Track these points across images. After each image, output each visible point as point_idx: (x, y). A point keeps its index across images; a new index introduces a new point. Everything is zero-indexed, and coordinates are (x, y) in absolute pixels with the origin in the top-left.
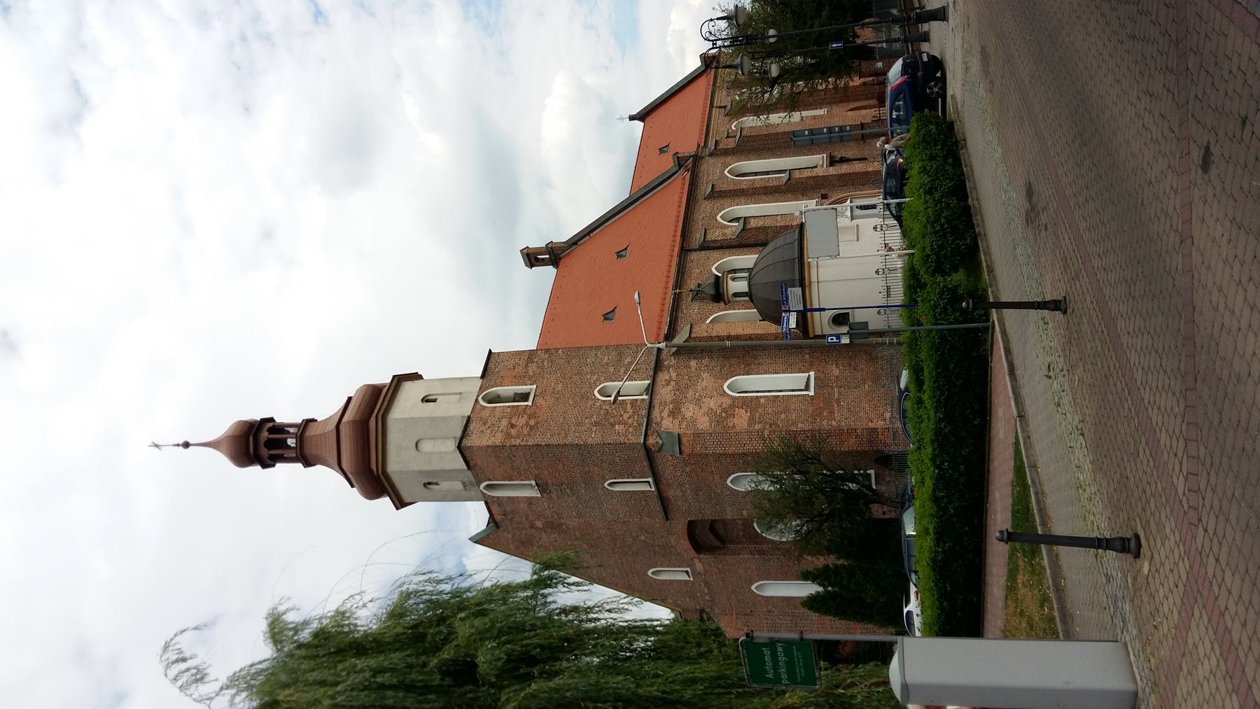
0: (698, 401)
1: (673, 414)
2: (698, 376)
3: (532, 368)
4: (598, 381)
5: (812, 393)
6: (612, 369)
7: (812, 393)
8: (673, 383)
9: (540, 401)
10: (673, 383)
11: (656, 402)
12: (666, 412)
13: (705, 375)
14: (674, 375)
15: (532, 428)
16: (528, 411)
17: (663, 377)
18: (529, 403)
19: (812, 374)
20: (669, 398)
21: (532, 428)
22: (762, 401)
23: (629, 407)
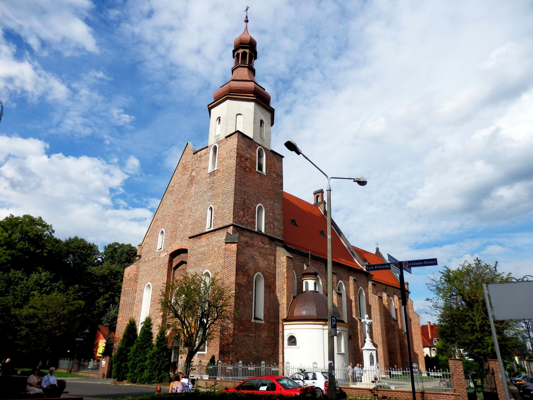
8: (263, 245)
11: (254, 235)
12: (248, 239)
17: (266, 240)
18: (257, 170)
19: (263, 322)
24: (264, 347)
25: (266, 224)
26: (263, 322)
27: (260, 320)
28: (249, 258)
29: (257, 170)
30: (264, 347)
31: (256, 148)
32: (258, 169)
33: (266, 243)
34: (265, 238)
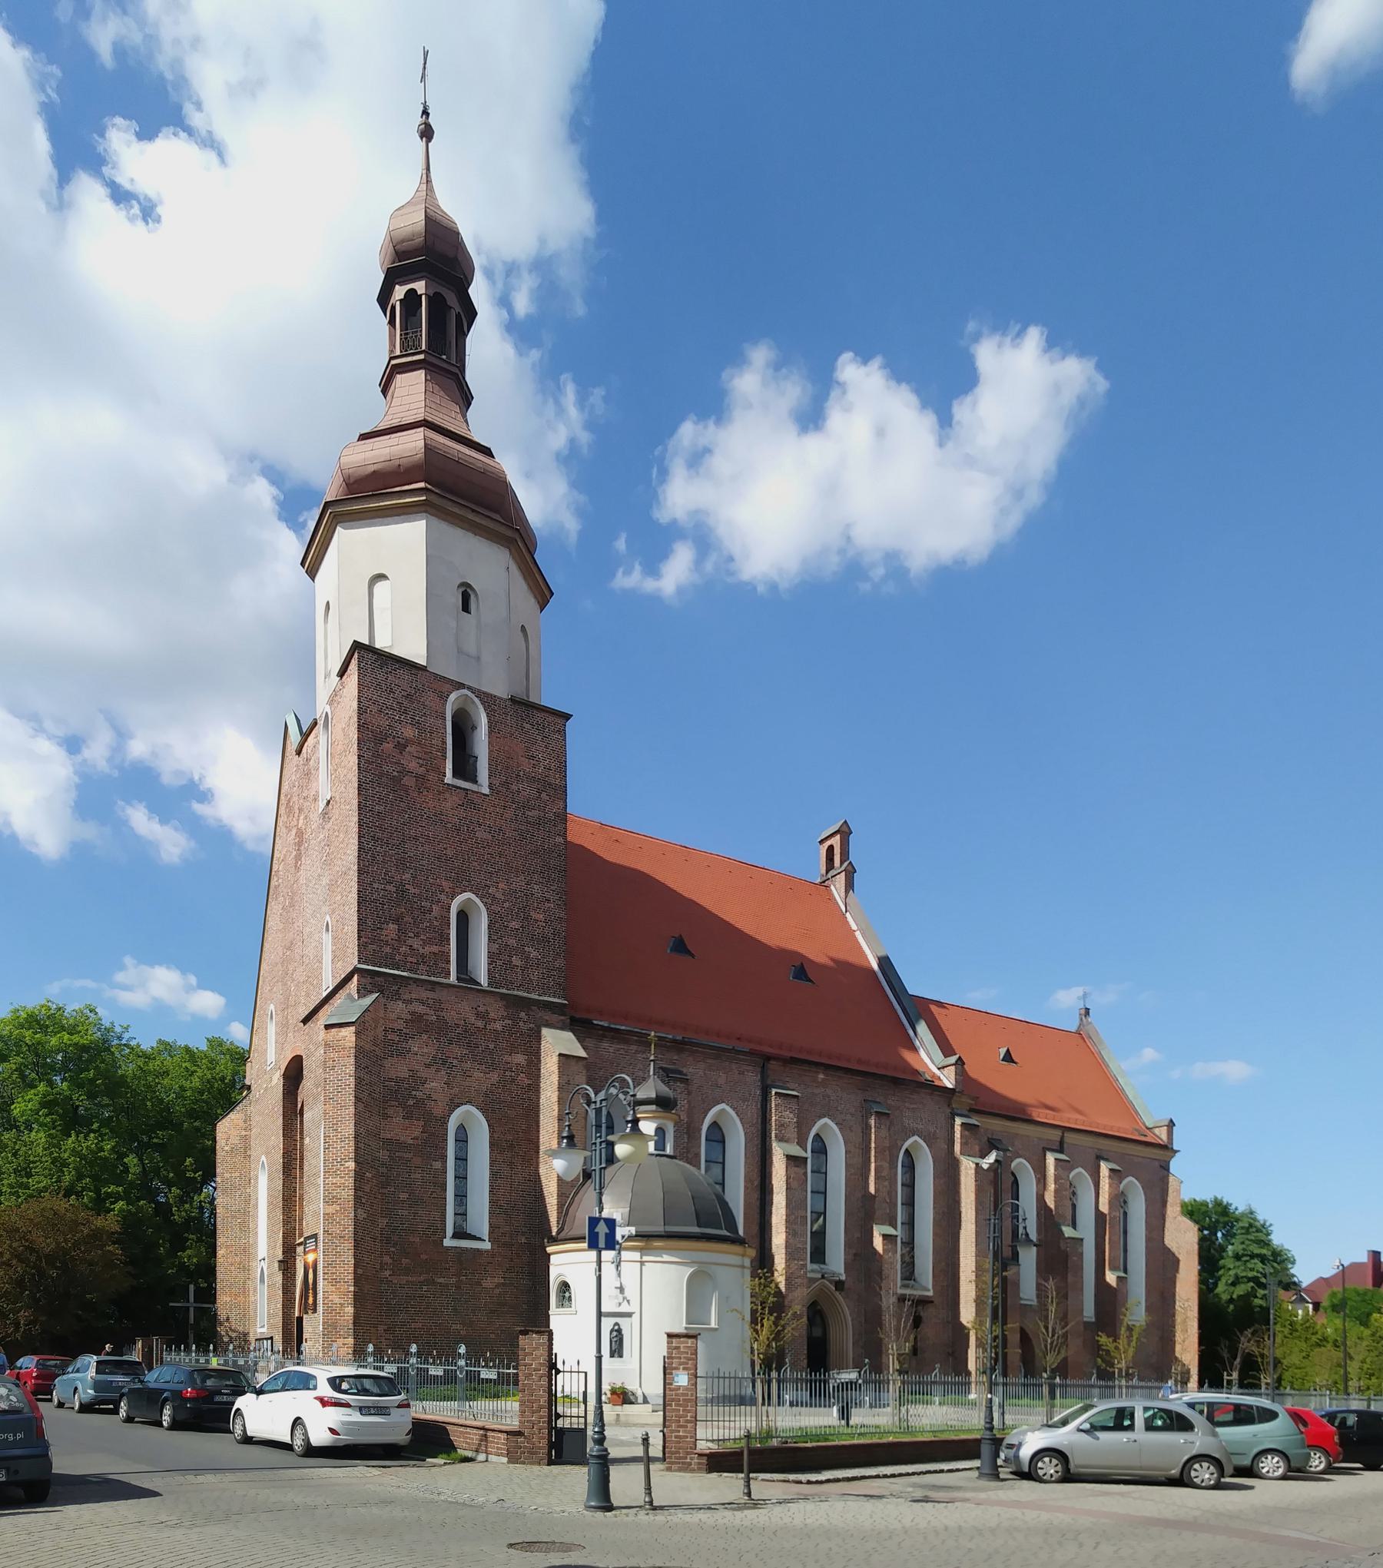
0: (441, 1062)
1: (416, 1019)
2: (493, 1067)
3: (527, 790)
4: (490, 902)
5: (448, 1242)
6: (514, 924)
7: (448, 1242)
8: (480, 1024)
9: (452, 801)
10: (480, 1024)
11: (442, 995)
12: (420, 1009)
13: (495, 1077)
14: (498, 1026)
15: (396, 781)
16: (432, 776)
18: (449, 778)
19: (487, 1246)
20: (451, 1016)
21: (396, 781)
22: (437, 1165)
23: (435, 949)
24: (492, 1312)
25: (491, 955)
26: (487, 1246)
27: (480, 1239)
28: (428, 1066)
29: (449, 778)
30: (492, 1312)
31: (444, 698)
32: (455, 774)
33: (492, 1015)
34: (489, 1000)
